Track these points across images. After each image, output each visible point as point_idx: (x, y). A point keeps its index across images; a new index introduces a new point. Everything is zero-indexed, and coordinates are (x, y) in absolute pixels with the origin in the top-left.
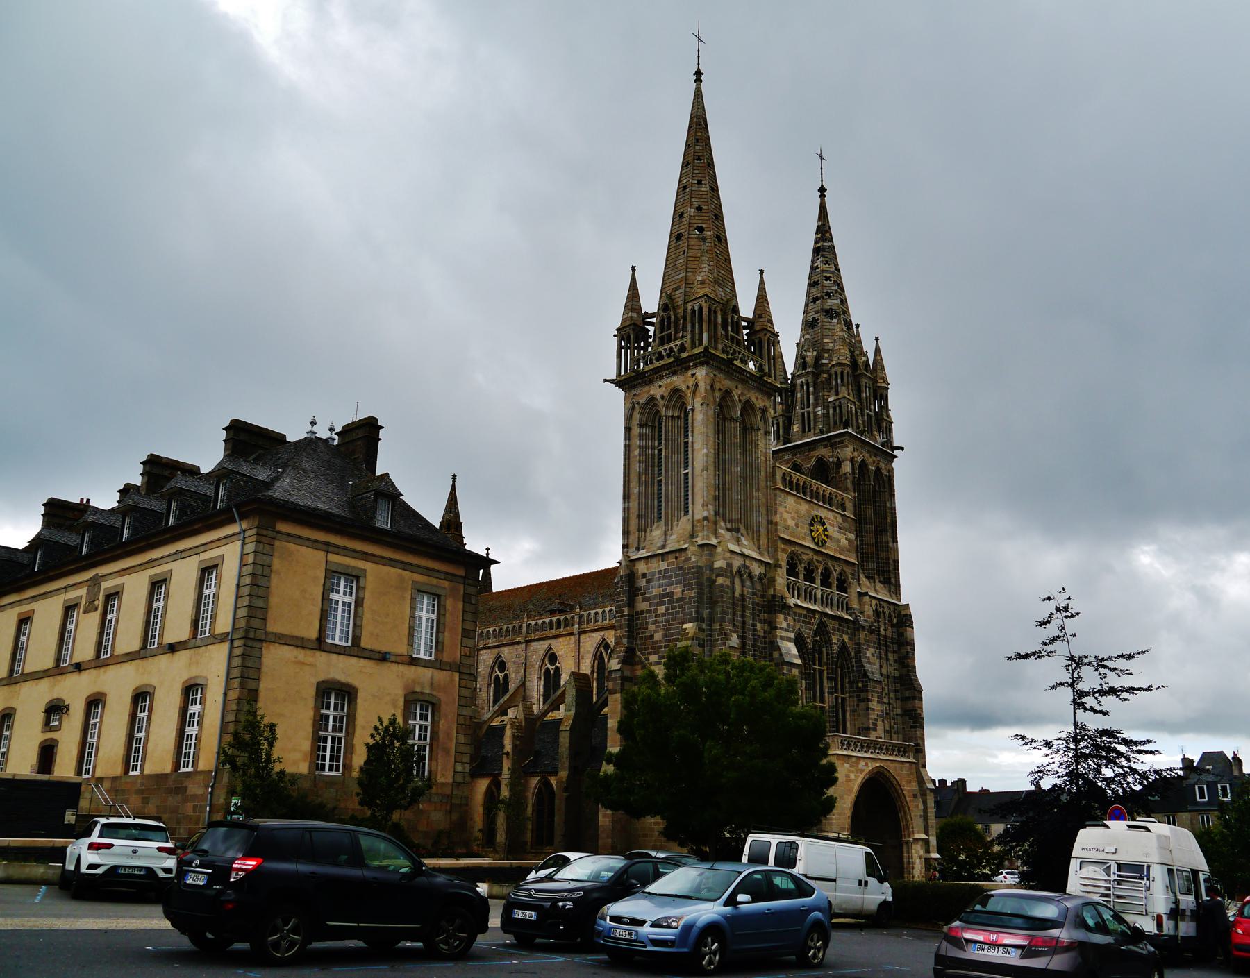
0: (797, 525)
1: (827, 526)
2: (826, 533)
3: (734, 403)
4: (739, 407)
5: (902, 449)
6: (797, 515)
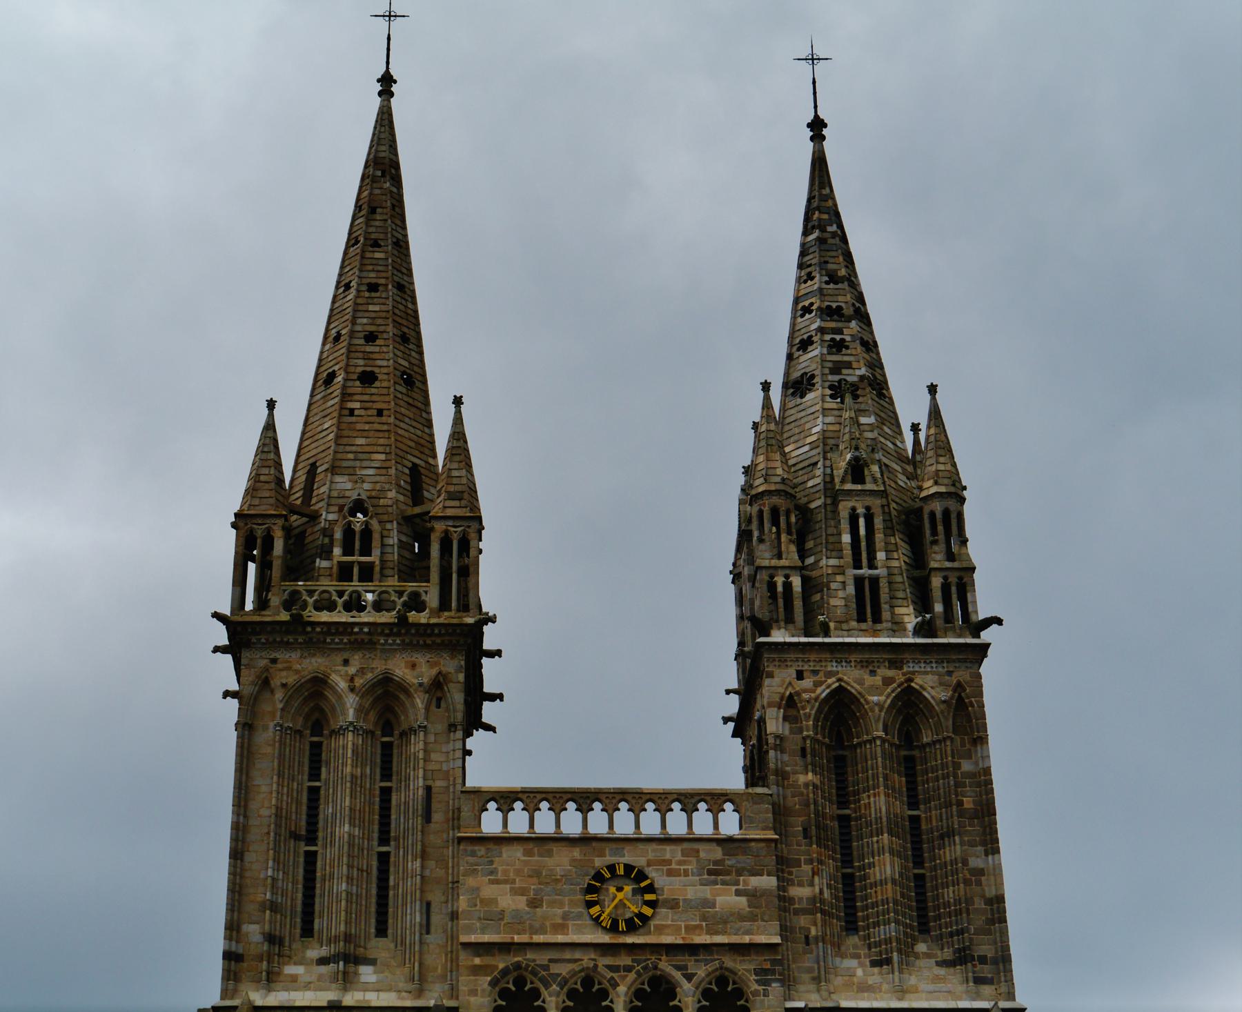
0: (534, 903)
1: (657, 876)
2: (648, 897)
3: (340, 697)
4: (351, 701)
5: (999, 621)
6: (535, 880)
